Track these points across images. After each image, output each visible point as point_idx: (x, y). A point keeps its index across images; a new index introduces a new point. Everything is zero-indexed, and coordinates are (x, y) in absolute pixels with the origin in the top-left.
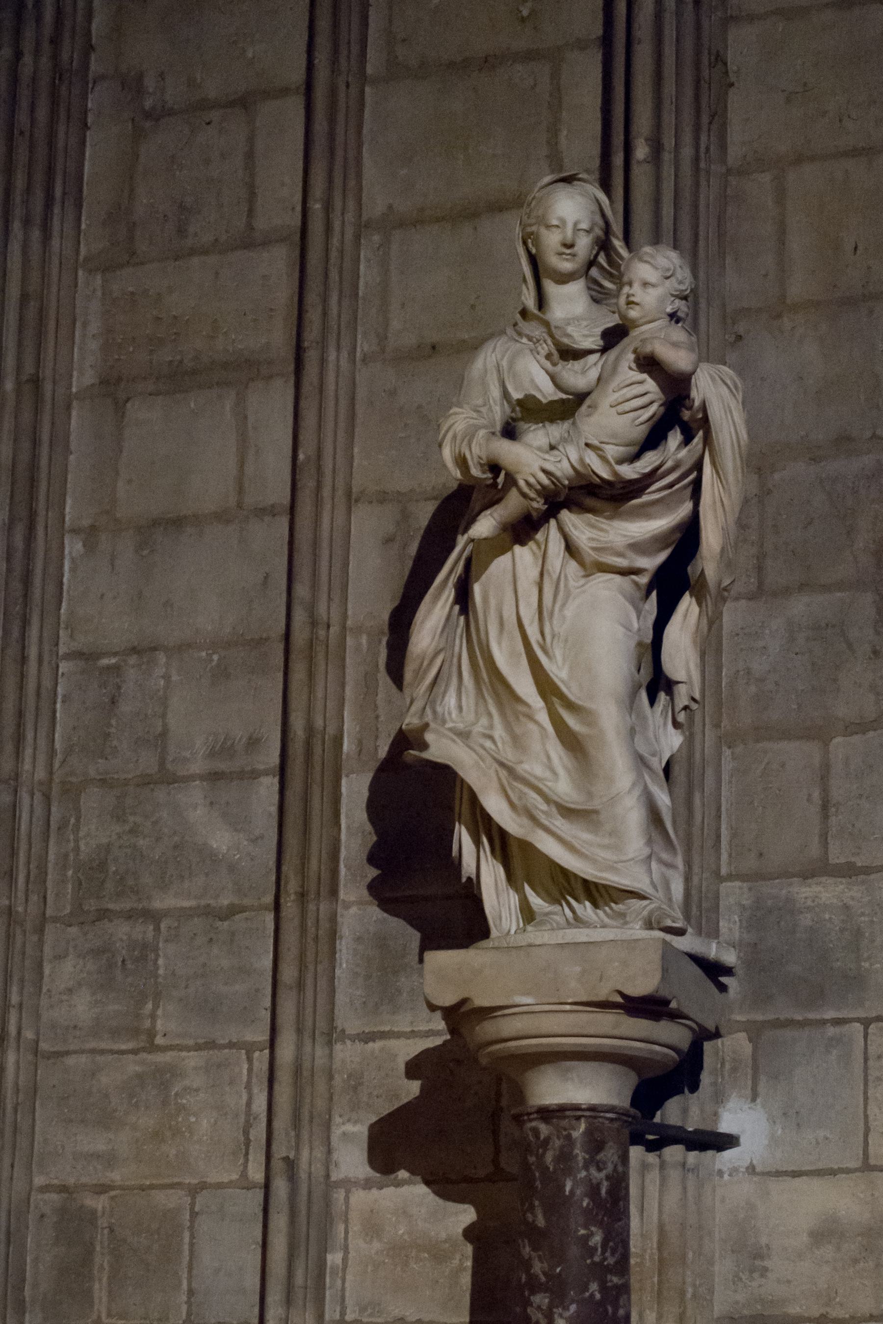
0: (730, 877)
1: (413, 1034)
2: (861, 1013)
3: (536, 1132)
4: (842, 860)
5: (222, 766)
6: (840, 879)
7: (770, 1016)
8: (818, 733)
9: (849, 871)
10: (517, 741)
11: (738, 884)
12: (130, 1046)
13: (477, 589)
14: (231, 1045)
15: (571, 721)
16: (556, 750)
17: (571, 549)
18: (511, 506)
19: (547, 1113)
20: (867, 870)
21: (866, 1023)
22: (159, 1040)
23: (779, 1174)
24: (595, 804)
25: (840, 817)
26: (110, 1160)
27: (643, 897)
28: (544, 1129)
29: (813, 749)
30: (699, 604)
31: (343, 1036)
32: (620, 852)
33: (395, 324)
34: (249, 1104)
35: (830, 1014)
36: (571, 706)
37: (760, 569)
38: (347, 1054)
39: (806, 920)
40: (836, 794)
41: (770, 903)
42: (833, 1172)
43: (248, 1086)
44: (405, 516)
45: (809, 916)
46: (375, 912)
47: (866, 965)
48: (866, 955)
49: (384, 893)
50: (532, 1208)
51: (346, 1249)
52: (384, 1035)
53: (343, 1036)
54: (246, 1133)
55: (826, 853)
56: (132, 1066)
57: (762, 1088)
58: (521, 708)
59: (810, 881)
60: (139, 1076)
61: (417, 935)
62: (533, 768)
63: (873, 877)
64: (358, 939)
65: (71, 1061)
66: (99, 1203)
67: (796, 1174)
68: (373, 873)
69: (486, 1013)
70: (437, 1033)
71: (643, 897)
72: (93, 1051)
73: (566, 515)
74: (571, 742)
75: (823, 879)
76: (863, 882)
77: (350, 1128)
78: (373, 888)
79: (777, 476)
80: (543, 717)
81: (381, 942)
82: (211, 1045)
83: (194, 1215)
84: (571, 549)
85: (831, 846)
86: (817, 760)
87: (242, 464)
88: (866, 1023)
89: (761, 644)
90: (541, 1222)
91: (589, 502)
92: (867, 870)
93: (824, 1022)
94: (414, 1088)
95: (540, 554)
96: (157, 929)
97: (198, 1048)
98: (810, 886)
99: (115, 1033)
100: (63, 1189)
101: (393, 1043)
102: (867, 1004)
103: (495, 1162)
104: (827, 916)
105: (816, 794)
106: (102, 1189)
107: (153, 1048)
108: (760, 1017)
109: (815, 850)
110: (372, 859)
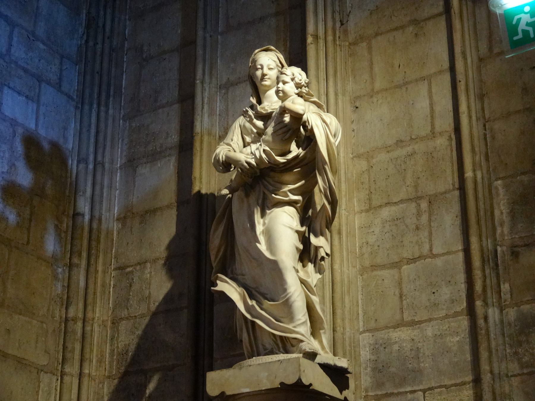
0: (364, 332)
2: (421, 387)
4: (410, 319)
6: (408, 328)
7: (384, 392)
8: (396, 265)
9: (412, 324)
11: (367, 334)
20: (420, 322)
25: (408, 300)
29: (394, 272)
35: (409, 389)
37: (370, 199)
39: (396, 347)
40: (405, 291)
41: (381, 341)
45: (397, 345)
47: (422, 365)
48: (422, 360)
55: (403, 317)
59: (396, 330)
63: (422, 325)
75: (402, 328)
76: (419, 328)
79: (374, 161)
85: (404, 314)
88: (424, 391)
89: (372, 230)
92: (420, 322)
93: (406, 392)
98: (397, 332)
102: (424, 383)
104: (405, 345)
105: (397, 293)
108: (380, 393)
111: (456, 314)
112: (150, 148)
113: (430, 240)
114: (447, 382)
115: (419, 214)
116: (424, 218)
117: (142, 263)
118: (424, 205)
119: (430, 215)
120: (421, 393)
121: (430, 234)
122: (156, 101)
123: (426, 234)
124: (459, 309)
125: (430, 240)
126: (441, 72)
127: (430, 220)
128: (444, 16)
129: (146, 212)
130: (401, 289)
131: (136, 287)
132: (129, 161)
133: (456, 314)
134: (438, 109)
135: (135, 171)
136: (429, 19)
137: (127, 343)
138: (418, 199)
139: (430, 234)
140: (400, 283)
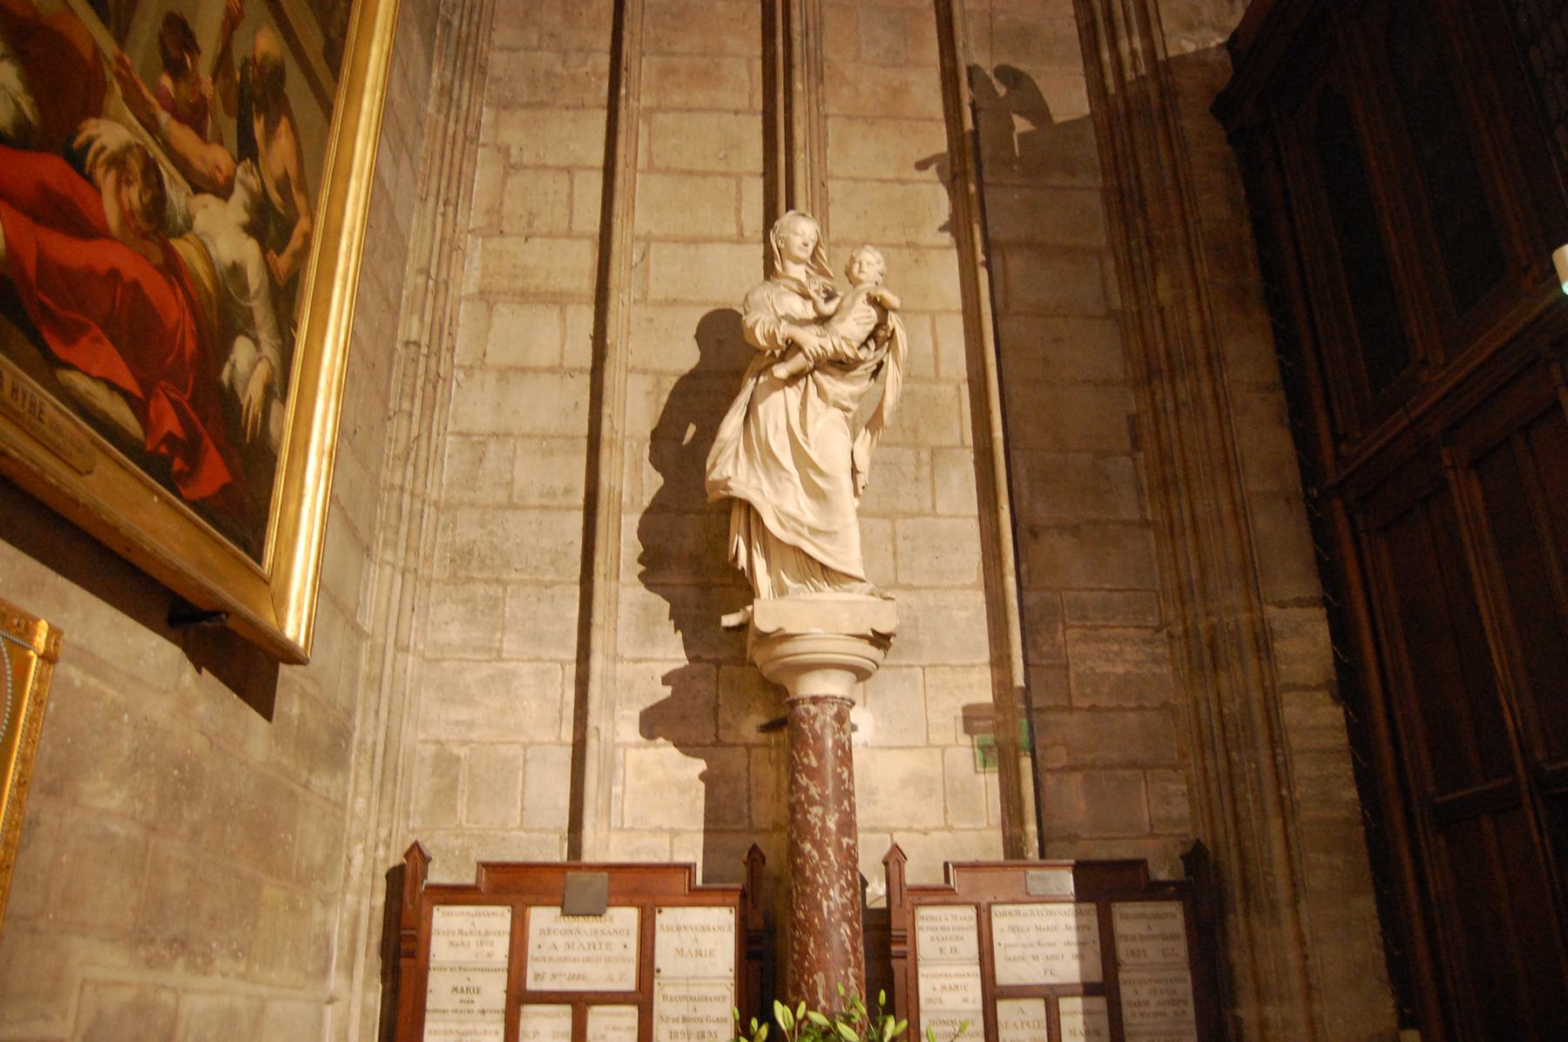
1: (665, 660)
3: (808, 711)
5: (547, 502)
10: (777, 491)
12: (486, 657)
13: (761, 409)
14: (551, 660)
15: (820, 482)
16: (804, 500)
17: (821, 393)
18: (797, 362)
19: (815, 700)
20: (919, 588)
21: (924, 668)
22: (504, 655)
23: (881, 748)
24: (835, 528)
26: (470, 725)
27: (862, 581)
28: (813, 709)
30: (872, 434)
31: (622, 659)
32: (846, 554)
33: (653, 287)
34: (562, 696)
35: (904, 662)
36: (821, 473)
38: (624, 670)
42: (910, 748)
43: (562, 685)
44: (659, 383)
46: (642, 589)
49: (648, 580)
50: (807, 755)
51: (624, 784)
52: (647, 660)
53: (622, 659)
54: (560, 712)
56: (486, 670)
57: (869, 699)
58: (783, 474)
60: (492, 677)
61: (668, 605)
62: (790, 508)
64: (631, 605)
65: (445, 665)
66: (462, 752)
67: (890, 748)
68: (641, 568)
69: (789, 637)
70: (678, 660)
71: (862, 581)
72: (461, 659)
73: (817, 373)
74: (817, 494)
77: (626, 712)
78: (641, 576)
80: (797, 480)
81: (646, 608)
82: (538, 659)
83: (525, 761)
84: (821, 393)
86: (889, 530)
87: (563, 345)
90: (814, 763)
91: (830, 369)
92: (919, 588)
94: (667, 691)
95: (800, 394)
96: (505, 590)
97: (530, 660)
99: (475, 650)
100: (438, 742)
101: (653, 665)
103: (717, 735)
105: (890, 547)
106: (465, 743)
107: (500, 659)
109: (891, 576)
110: (640, 561)
111: (964, 587)
112: (519, 284)
113: (933, 496)
114: (953, 662)
115: (918, 463)
116: (926, 470)
117: (502, 436)
118: (925, 455)
119: (932, 468)
120: (920, 670)
121: (933, 490)
122: (530, 224)
123: (928, 488)
124: (968, 582)
125: (933, 496)
126: (947, 311)
127: (933, 474)
128: (954, 253)
129: (509, 368)
130: (895, 546)
131: (489, 464)
132: (481, 293)
133: (964, 587)
134: (943, 351)
135: (490, 307)
136: (933, 247)
137: (472, 537)
138: (917, 447)
139: (933, 490)
140: (894, 539)
